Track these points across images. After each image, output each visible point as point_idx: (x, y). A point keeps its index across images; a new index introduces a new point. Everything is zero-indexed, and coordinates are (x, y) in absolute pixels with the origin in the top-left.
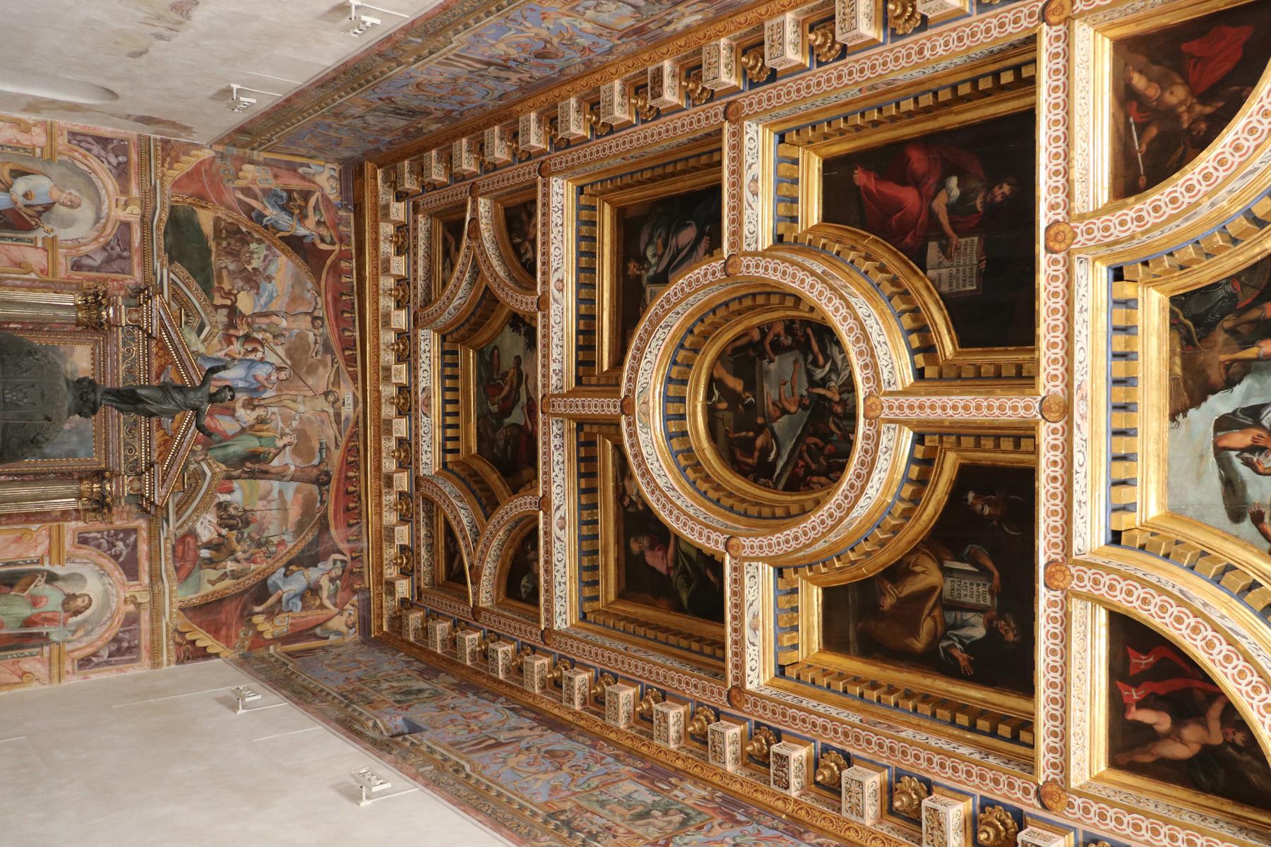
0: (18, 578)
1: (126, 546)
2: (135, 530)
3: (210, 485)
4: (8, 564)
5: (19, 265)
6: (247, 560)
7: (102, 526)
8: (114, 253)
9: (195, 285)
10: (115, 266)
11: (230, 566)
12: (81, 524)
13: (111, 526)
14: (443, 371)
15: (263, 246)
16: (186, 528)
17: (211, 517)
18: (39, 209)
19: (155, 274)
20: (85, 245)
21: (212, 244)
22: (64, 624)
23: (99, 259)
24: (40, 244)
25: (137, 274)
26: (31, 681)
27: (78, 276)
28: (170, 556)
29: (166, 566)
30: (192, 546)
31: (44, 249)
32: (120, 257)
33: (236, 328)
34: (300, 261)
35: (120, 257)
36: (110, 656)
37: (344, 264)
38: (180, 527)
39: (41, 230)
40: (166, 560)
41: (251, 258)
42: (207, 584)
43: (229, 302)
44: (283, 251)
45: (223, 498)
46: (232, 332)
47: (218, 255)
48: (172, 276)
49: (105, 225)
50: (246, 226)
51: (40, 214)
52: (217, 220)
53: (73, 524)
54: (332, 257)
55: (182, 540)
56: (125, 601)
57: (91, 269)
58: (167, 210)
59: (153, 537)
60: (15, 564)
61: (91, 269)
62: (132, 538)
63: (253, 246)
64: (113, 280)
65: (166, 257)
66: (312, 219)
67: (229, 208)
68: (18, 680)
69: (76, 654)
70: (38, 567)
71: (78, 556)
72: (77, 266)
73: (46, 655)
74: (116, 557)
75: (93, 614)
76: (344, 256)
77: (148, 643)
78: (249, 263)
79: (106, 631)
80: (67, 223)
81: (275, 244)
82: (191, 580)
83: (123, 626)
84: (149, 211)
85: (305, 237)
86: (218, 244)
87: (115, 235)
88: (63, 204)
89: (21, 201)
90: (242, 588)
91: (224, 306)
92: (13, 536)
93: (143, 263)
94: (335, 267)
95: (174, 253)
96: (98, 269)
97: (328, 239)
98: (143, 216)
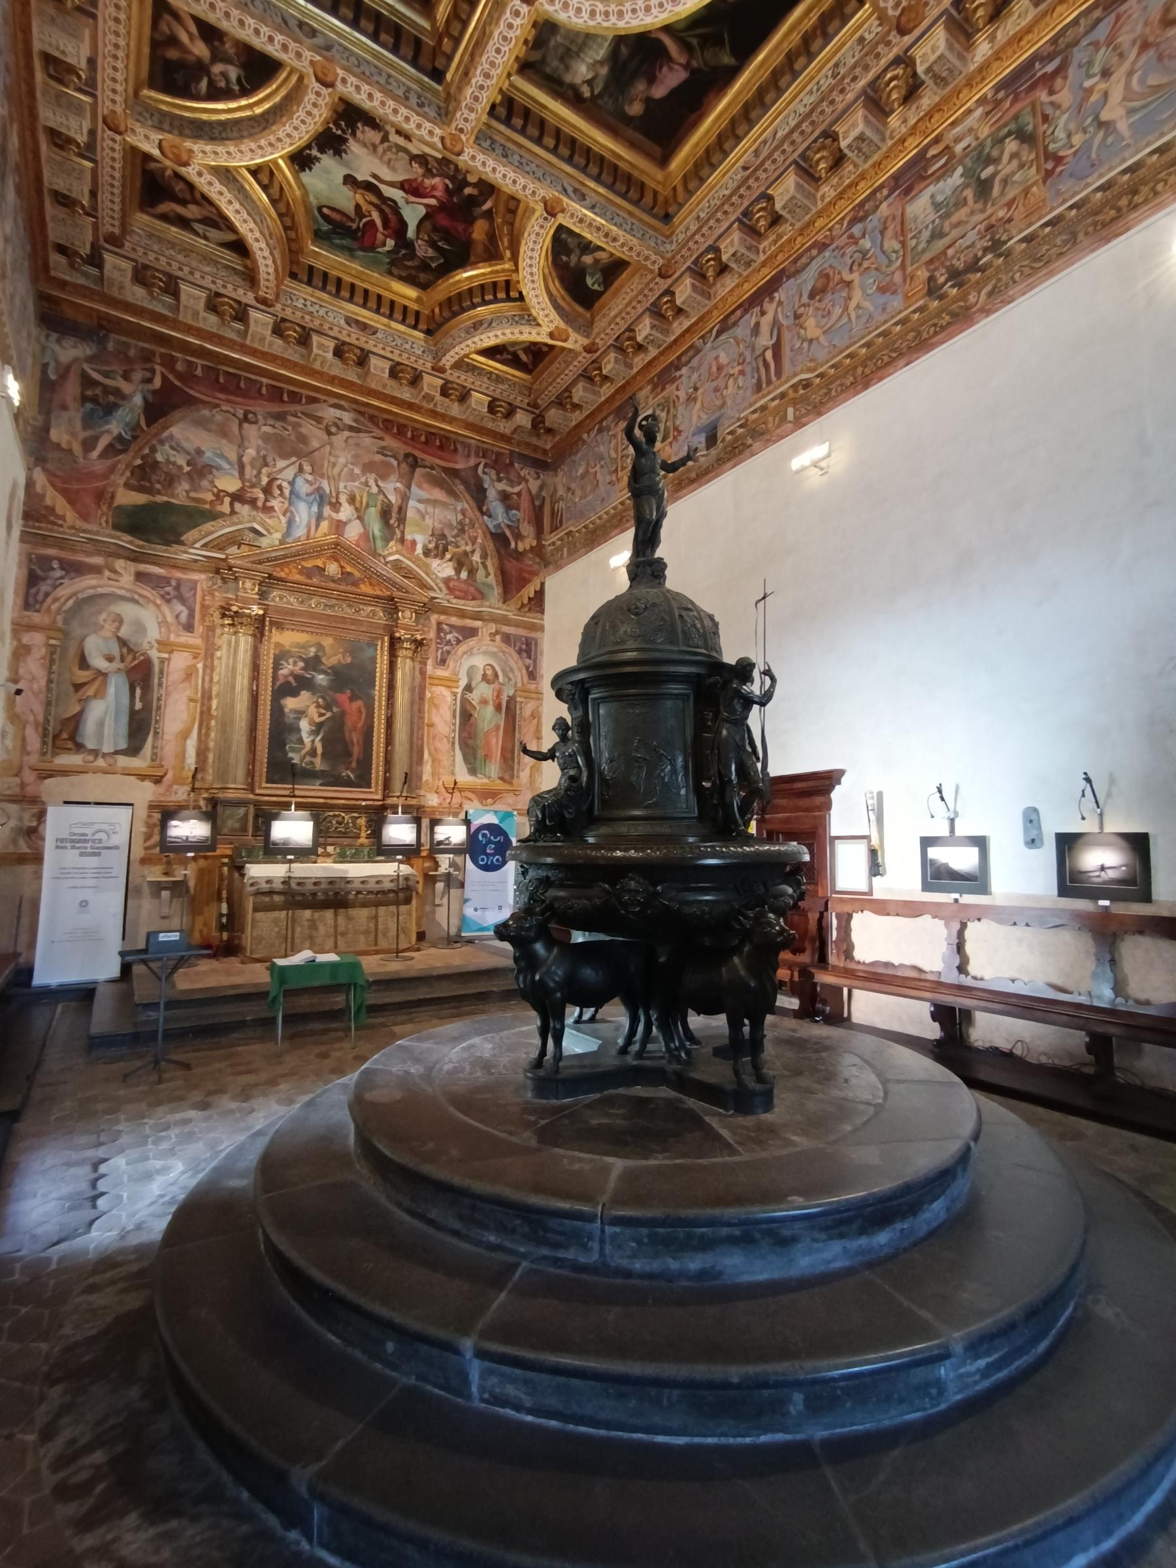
2: (439, 624)
6: (473, 544)
8: (173, 593)
11: (476, 558)
14: (329, 293)
15: (159, 447)
16: (442, 585)
17: (435, 564)
18: (125, 650)
19: (196, 561)
20: (164, 617)
21: (160, 499)
23: (179, 607)
24: (166, 656)
25: (195, 576)
27: (199, 629)
29: (470, 606)
30: (457, 584)
31: (171, 652)
32: (177, 588)
34: (177, 414)
35: (177, 588)
37: (180, 367)
41: (174, 464)
42: (488, 577)
44: (166, 428)
47: (172, 496)
49: (141, 595)
50: (134, 458)
51: (130, 650)
52: (127, 486)
54: (171, 377)
55: (451, 590)
57: (191, 615)
58: (119, 534)
59: (444, 611)
61: (191, 615)
63: (159, 457)
64: (203, 599)
65: (176, 547)
66: (121, 383)
67: (112, 469)
72: (189, 627)
76: (169, 362)
78: (180, 468)
80: (140, 628)
81: (156, 435)
82: (485, 590)
84: (121, 552)
85: (145, 399)
86: (159, 492)
87: (153, 588)
88: (118, 628)
89: (117, 665)
90: (495, 553)
94: (179, 376)
95: (172, 538)
97: (148, 375)
98: (128, 558)
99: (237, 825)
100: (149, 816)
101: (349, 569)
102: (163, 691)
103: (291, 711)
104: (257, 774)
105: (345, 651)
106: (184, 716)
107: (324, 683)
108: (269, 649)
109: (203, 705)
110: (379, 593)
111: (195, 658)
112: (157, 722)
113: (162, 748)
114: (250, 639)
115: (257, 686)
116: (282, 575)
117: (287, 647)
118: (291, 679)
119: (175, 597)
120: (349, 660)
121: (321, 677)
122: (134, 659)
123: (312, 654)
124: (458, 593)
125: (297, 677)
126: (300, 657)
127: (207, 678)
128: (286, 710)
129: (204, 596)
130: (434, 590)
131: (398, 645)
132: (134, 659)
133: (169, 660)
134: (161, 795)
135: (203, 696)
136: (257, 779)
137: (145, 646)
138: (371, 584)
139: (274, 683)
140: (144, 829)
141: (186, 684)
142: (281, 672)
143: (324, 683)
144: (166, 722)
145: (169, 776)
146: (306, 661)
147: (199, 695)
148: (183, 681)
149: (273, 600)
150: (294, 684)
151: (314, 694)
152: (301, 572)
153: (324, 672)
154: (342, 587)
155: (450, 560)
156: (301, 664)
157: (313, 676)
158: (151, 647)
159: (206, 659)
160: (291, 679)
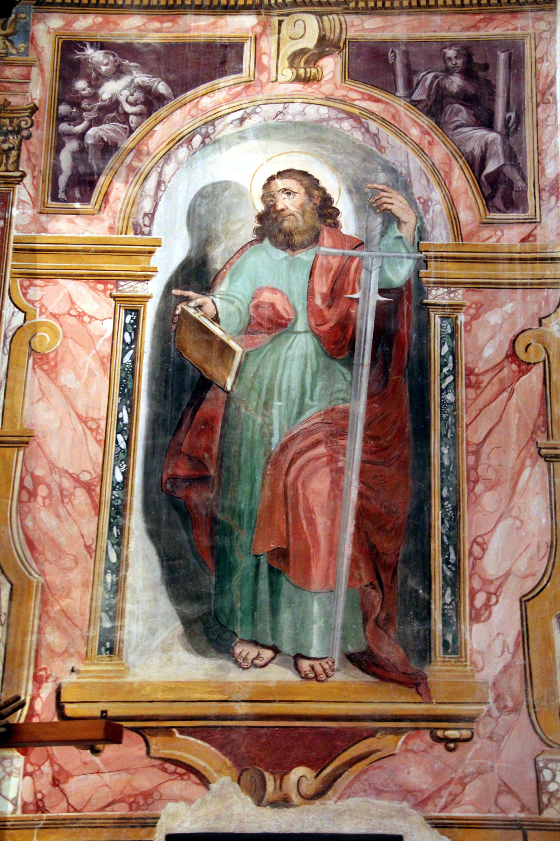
0: (181, 367)
22: (359, 245)
26: (541, 339)
36: (490, 125)
56: (306, 80)
68: (536, 374)
69: (465, 216)
71: (134, 203)
73: (459, 296)
75: (336, 168)
77: (469, 20)
79: (402, 134)
83: (390, 89)
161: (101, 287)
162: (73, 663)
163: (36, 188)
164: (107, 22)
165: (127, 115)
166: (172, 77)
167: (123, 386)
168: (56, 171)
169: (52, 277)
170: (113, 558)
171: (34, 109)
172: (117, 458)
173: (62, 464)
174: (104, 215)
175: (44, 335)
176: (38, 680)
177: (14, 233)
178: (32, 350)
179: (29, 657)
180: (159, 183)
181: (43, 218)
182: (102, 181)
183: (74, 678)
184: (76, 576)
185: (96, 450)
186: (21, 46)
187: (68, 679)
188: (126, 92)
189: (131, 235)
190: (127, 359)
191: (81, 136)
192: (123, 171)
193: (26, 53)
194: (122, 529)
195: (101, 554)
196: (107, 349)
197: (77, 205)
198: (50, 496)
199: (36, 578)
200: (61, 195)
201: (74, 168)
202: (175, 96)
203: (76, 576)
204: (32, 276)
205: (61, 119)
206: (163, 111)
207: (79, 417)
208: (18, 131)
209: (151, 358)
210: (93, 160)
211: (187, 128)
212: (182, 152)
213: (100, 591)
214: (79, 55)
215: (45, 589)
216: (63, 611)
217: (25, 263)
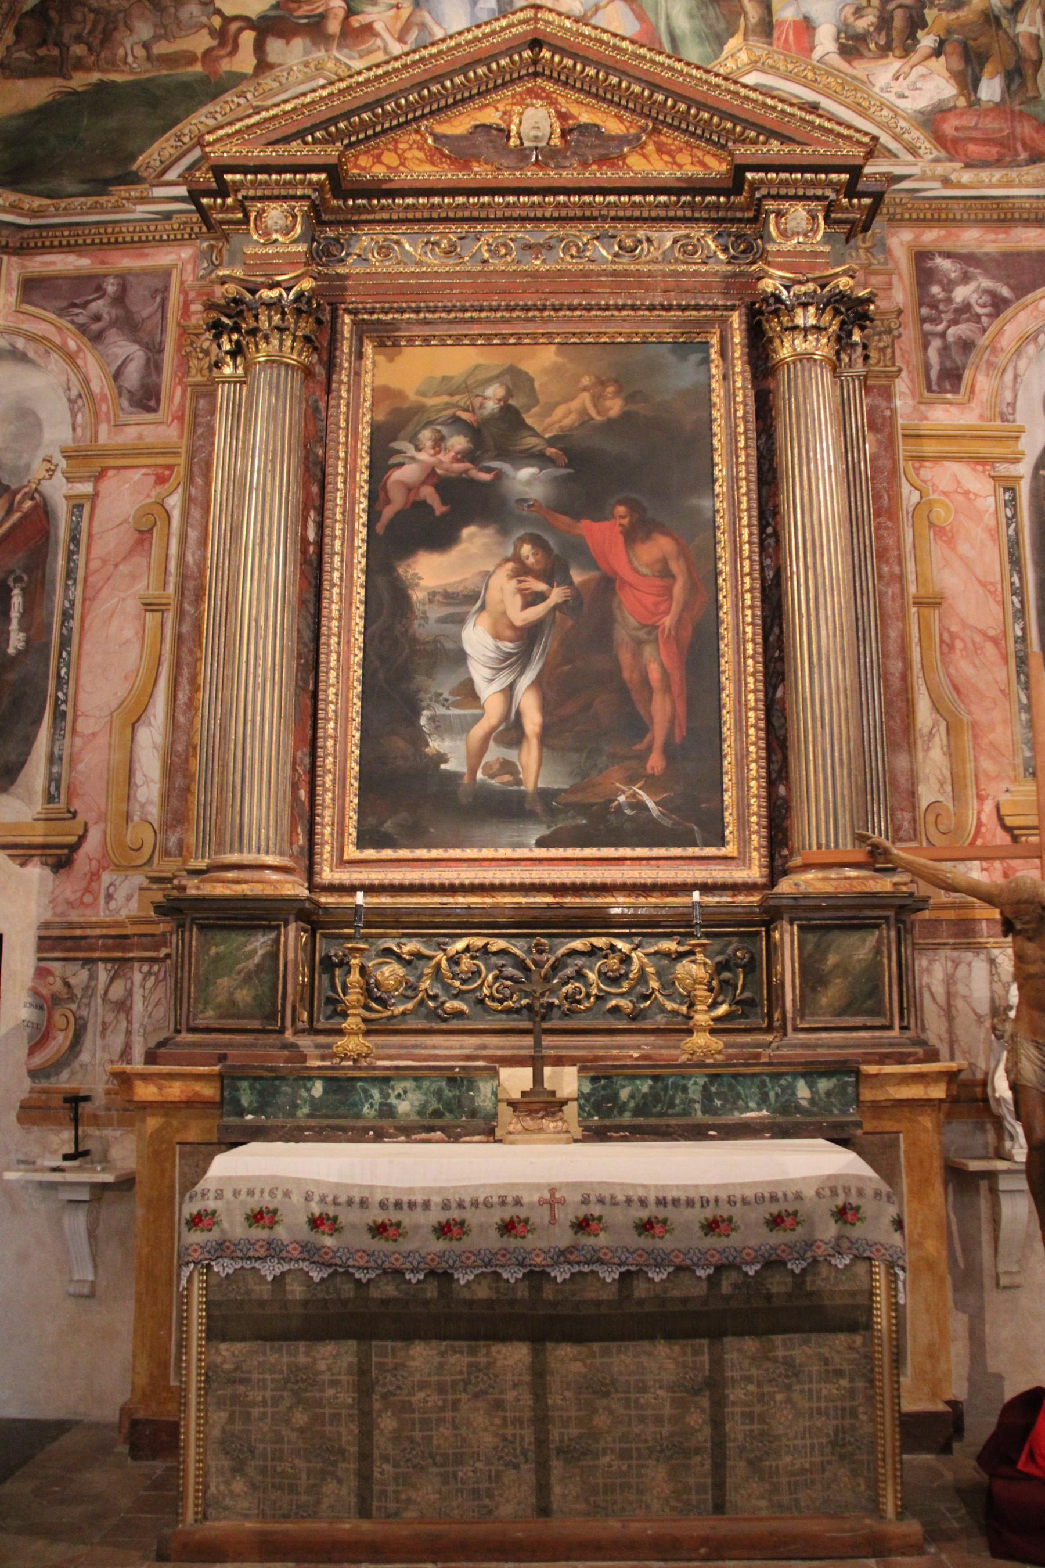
1: (966, 278)
2: (921, 257)
3: (788, 77)
4: (1016, 562)
5: (144, 535)
7: (909, 336)
9: (200, 119)
10: (144, 310)
12: (902, 385)
13: (908, 318)
16: (915, 134)
19: (168, 216)
20: (87, 382)
24: (87, 488)
28: (997, 175)
31: (99, 476)
32: (120, 300)
33: (323, 17)
35: (120, 300)
38: (913, 151)
39: (46, 487)
40: (1009, 184)
43: (248, 37)
45: (825, 42)
46: (333, 27)
48: (172, 175)
49: (31, 338)
53: (903, 403)
57: (153, 366)
60: (1015, 544)
61: (153, 366)
62: (945, 264)
64: (186, 313)
65: (122, 191)
70: (1024, 489)
71: (997, 394)
74: (998, 305)
87: (61, 313)
91: (259, 47)
92: (937, 550)
93: (139, 244)
95: (110, 172)
96: (154, 351)
99: (244, 996)
100: (41, 973)
101: (585, 118)
102: (77, 593)
103: (432, 595)
104: (326, 816)
105: (602, 383)
106: (132, 657)
107: (537, 493)
108: (354, 406)
109: (181, 614)
110: (698, 171)
111: (161, 480)
112: (61, 682)
113: (72, 762)
114: (292, 384)
115: (320, 526)
116: (379, 171)
117: (412, 397)
118: (428, 493)
119: (114, 323)
120: (615, 407)
121: (526, 473)
122: (9, 512)
123: (491, 406)
124: (972, 148)
125: (445, 485)
126: (456, 420)
127: (193, 534)
128: (417, 596)
129: (187, 304)
130: (891, 154)
131: (773, 326)
132: (9, 512)
133: (94, 497)
134: (70, 904)
135: (181, 590)
136: (326, 832)
137: (38, 469)
138: (661, 149)
139: (373, 513)
140: (25, 1013)
141: (139, 560)
142: (397, 475)
143: (537, 493)
144: (85, 679)
145: (92, 845)
146: (474, 431)
147: (171, 589)
148: (132, 552)
149: (363, 259)
150: (439, 509)
151: (504, 532)
152: (433, 156)
153: (539, 458)
154: (570, 176)
155: (937, 52)
156: (459, 442)
157: (499, 475)
158: (51, 472)
159: (191, 479)
160: (428, 493)
161: (980, 468)
162: (1005, 785)
163: (912, 380)
164: (950, 234)
165: (979, 316)
166: (1012, 282)
167: (1011, 554)
168: (927, 367)
169: (938, 459)
170: (1024, 700)
171: (900, 312)
172: (1015, 617)
173: (971, 621)
174: (973, 404)
175: (937, 509)
176: (981, 798)
177: (900, 421)
178: (931, 524)
179: (970, 781)
180: (1016, 377)
181: (923, 408)
182: (967, 375)
183: (1008, 796)
184: (997, 715)
185: (997, 610)
186: (881, 257)
187: (1003, 797)
188: (975, 296)
189: (999, 422)
190: (1011, 531)
191: (943, 335)
192: (983, 366)
193: (886, 263)
194: (1027, 676)
195: (1014, 698)
196: (992, 523)
197: (949, 396)
198: (965, 648)
199: (966, 718)
200: (935, 387)
201: (942, 363)
202: (1018, 298)
203: (997, 715)
204: (922, 459)
205: (924, 320)
206: (1009, 312)
207: (979, 581)
208: (889, 331)
209: (1032, 529)
210: (957, 357)
211: (1032, 327)
212: (1031, 349)
213: (1018, 728)
214: (930, 264)
215: (974, 725)
216: (991, 744)
217: (913, 447)
